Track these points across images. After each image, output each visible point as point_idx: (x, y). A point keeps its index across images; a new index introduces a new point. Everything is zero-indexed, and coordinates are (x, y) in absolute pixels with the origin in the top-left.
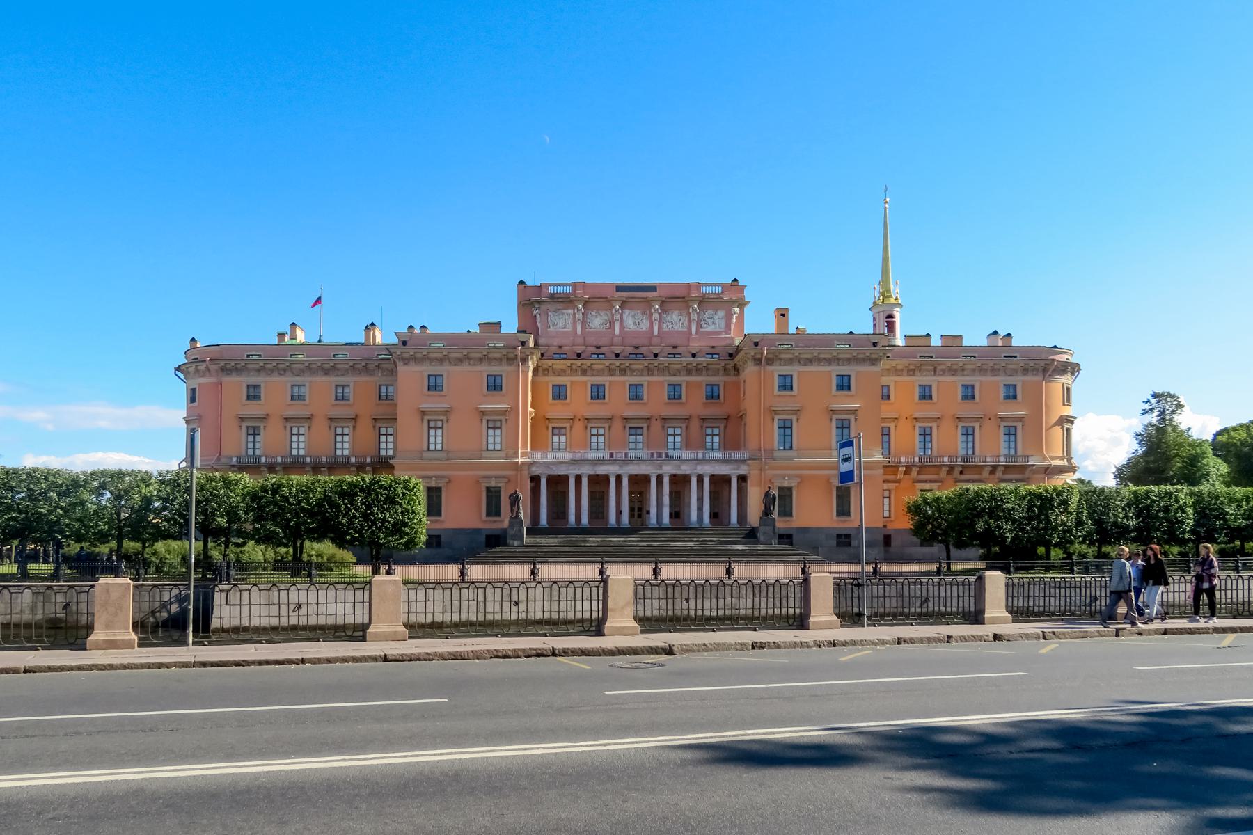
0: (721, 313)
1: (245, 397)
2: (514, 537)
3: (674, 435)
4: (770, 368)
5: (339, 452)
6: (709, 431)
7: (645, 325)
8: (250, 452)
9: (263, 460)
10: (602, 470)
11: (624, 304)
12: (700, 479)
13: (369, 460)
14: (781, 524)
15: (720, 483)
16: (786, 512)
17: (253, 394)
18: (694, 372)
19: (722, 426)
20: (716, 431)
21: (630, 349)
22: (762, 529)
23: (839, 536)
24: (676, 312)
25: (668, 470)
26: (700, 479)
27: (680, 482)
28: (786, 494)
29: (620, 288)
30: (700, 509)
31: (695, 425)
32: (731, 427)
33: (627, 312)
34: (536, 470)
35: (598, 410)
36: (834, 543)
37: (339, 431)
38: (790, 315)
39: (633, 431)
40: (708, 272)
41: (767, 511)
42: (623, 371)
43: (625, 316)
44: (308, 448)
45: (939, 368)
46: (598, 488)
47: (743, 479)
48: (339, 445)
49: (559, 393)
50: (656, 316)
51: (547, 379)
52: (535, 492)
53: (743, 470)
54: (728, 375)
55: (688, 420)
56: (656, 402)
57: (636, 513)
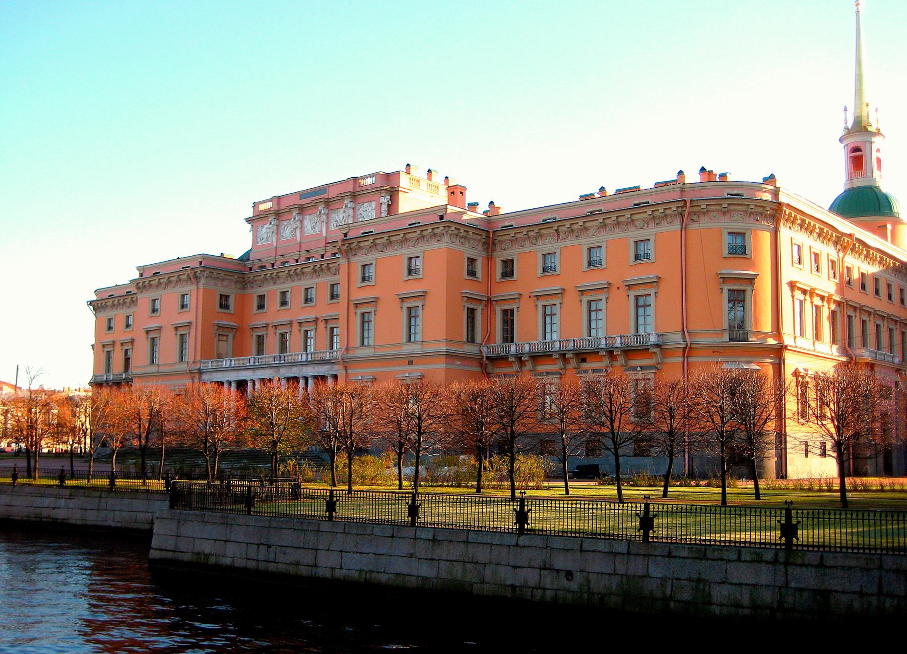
0: (374, 204)
1: (106, 329)
4: (353, 259)
7: (317, 230)
11: (302, 209)
21: (304, 255)
24: (342, 210)
29: (303, 194)
33: (308, 217)
35: (283, 318)
38: (467, 193)
40: (364, 165)
42: (298, 274)
45: (561, 229)
50: (324, 217)
51: (253, 291)
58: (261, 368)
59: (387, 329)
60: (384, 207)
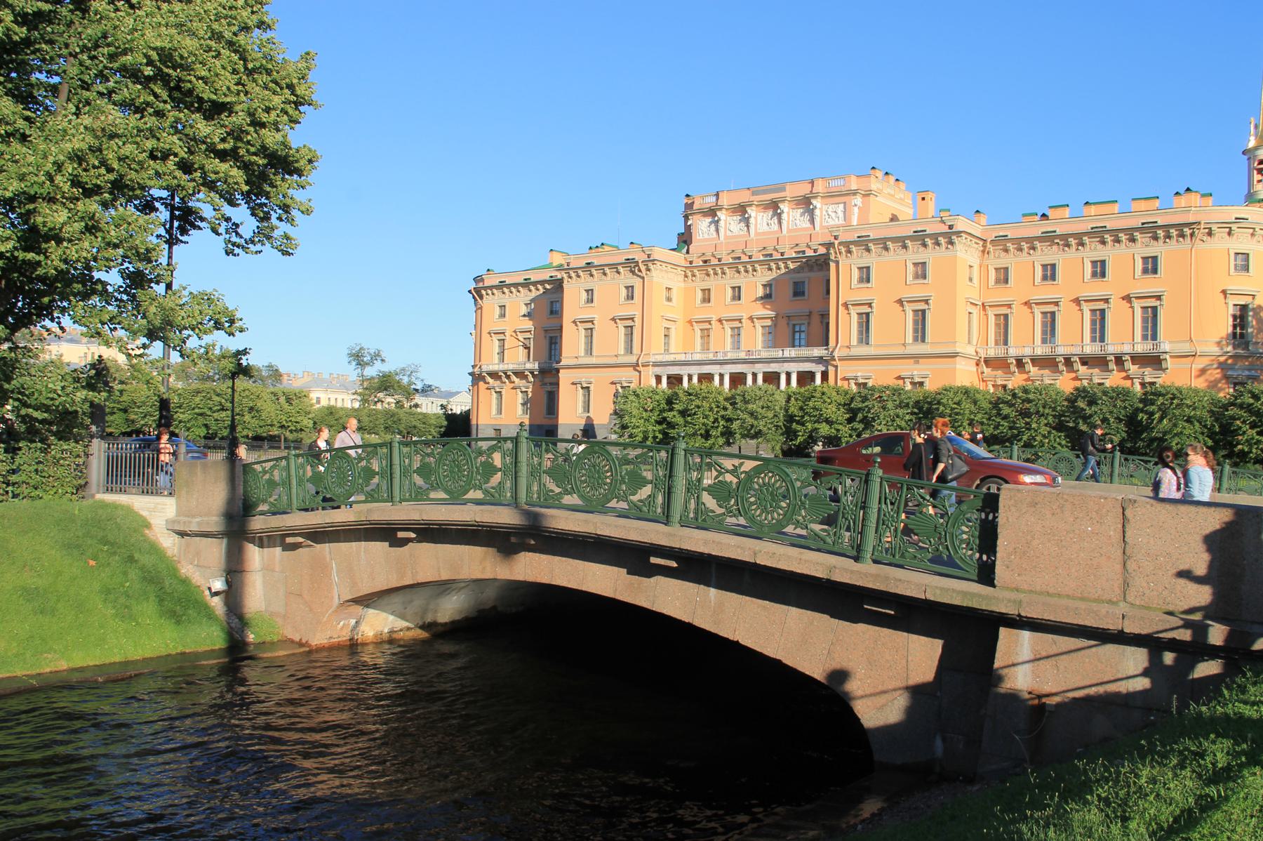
4: (848, 262)
12: (788, 375)
18: (816, 268)
26: (788, 375)
34: (658, 370)
43: (759, 218)
60: (856, 209)
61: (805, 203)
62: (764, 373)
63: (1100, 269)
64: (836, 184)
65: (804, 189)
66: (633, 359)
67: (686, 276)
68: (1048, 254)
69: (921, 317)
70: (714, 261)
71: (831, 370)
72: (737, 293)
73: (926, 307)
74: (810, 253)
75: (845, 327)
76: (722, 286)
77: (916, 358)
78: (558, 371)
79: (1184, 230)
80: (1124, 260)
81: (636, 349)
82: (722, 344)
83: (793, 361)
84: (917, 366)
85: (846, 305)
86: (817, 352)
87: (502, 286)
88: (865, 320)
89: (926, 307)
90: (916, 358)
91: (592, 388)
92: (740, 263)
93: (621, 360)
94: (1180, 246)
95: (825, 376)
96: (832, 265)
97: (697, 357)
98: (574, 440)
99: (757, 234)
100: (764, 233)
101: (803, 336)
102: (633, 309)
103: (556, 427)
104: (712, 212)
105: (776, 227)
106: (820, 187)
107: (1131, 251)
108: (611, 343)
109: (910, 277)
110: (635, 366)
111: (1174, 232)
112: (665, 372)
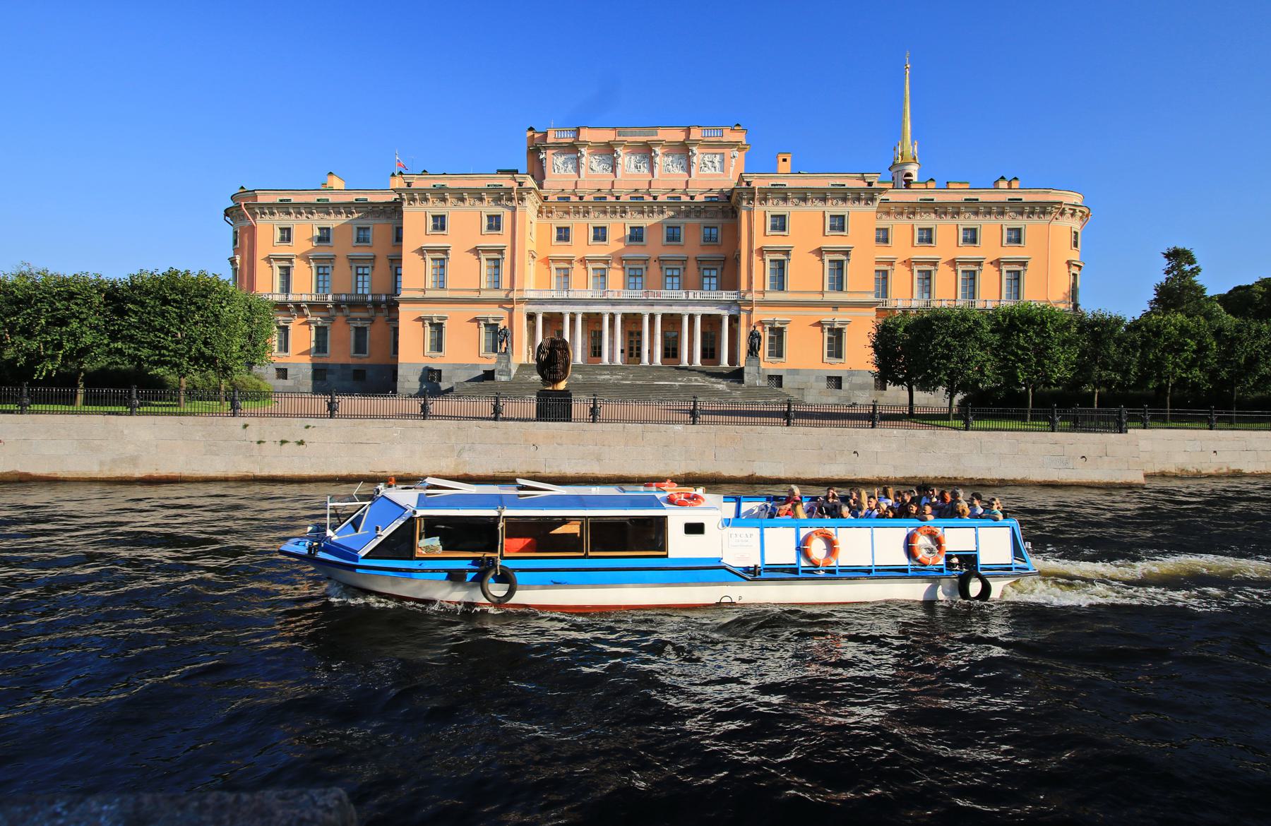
2: (502, 372)
3: (672, 276)
4: (764, 208)
5: (360, 291)
6: (707, 273)
8: (360, 291)
9: (370, 298)
10: (594, 309)
13: (384, 298)
14: (768, 364)
15: (711, 323)
16: (777, 351)
17: (286, 234)
19: (719, 268)
20: (714, 273)
22: (746, 370)
23: (829, 378)
25: (659, 310)
27: (672, 322)
28: (778, 334)
30: (651, 352)
31: (692, 266)
32: (724, 268)
35: (601, 251)
36: (824, 384)
37: (360, 271)
39: (632, 273)
41: (753, 351)
44: (371, 288)
46: (633, 328)
47: (734, 320)
48: (360, 285)
49: (564, 234)
52: (532, 330)
53: (733, 312)
54: (726, 217)
55: (684, 261)
56: (655, 246)
57: (635, 352)
58: (630, 302)
59: (806, 275)
61: (683, 150)
62: (664, 315)
63: (972, 237)
64: (713, 136)
65: (679, 136)
66: (501, 295)
67: (540, 212)
68: (928, 220)
69: (839, 267)
70: (573, 199)
71: (743, 316)
72: (600, 234)
73: (785, 257)
74: (685, 199)
75: (756, 274)
76: (581, 227)
77: (836, 306)
78: (397, 304)
79: (1042, 209)
80: (991, 229)
81: (505, 284)
82: (583, 287)
83: (697, 303)
84: (836, 313)
85: (761, 251)
86: (726, 296)
87: (285, 207)
88: (780, 267)
89: (785, 257)
90: (836, 306)
91: (446, 323)
92: (604, 203)
93: (484, 295)
94: (1040, 222)
95: (734, 320)
96: (744, 214)
97: (555, 295)
98: (862, 387)
99: (624, 175)
100: (632, 175)
101: (676, 280)
102: (500, 240)
103: (396, 366)
104: (572, 149)
105: (645, 170)
106: (696, 134)
107: (1000, 222)
108: (466, 274)
109: (828, 228)
110: (501, 303)
111: (1038, 209)
112: (540, 310)
